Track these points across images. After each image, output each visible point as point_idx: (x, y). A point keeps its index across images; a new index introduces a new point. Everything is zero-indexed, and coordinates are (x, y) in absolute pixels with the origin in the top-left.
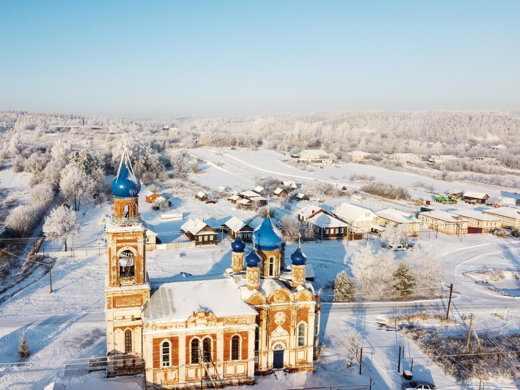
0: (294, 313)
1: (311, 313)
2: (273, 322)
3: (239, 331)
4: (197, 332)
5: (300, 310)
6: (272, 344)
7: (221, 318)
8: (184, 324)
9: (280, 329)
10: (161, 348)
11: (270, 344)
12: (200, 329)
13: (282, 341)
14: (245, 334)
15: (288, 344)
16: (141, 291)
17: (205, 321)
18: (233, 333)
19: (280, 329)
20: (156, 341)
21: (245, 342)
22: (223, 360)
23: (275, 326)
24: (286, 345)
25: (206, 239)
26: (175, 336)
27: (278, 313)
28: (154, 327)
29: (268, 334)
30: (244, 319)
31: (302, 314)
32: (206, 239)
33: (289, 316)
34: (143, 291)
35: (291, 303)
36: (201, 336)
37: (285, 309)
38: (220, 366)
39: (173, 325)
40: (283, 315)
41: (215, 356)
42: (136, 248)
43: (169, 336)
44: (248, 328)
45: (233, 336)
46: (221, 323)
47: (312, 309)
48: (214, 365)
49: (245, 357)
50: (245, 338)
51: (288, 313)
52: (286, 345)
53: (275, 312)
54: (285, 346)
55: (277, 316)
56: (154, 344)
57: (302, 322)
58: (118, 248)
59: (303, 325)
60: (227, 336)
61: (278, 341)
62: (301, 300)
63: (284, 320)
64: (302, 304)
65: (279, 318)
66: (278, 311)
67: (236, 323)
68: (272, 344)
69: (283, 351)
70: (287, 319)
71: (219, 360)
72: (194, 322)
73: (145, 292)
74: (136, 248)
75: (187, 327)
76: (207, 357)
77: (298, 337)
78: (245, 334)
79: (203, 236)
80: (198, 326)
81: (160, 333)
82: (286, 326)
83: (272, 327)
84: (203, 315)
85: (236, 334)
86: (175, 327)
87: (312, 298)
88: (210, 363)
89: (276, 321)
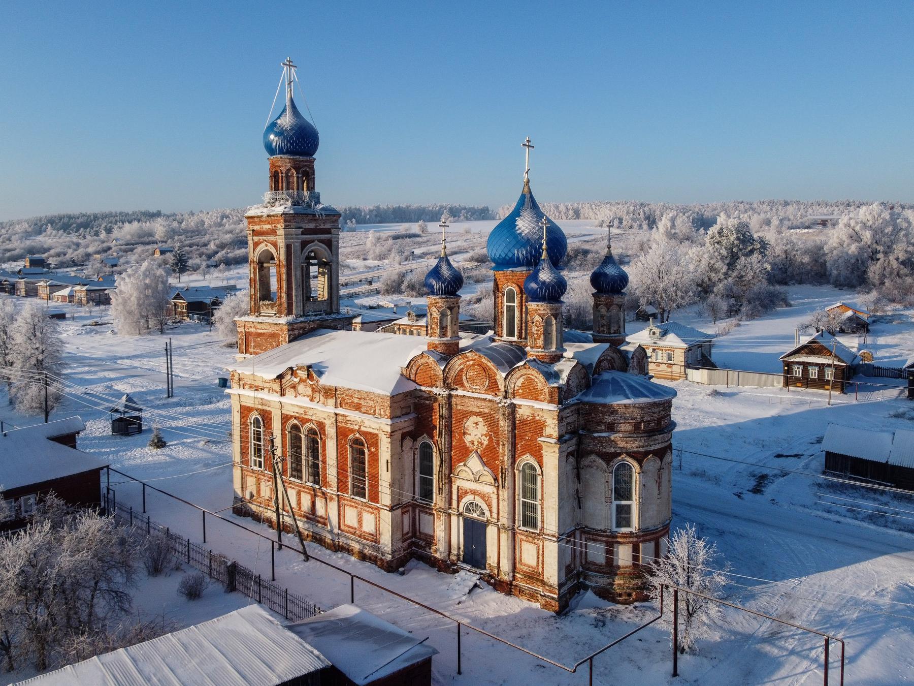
0: (504, 425)
1: (550, 436)
2: (461, 440)
3: (363, 429)
4: (296, 410)
5: (524, 422)
6: (459, 499)
7: (330, 390)
8: (276, 387)
9: (474, 463)
10: (252, 429)
11: (455, 497)
12: (296, 403)
13: (483, 496)
14: (373, 439)
15: (495, 510)
16: (277, 328)
17: (309, 391)
18: (352, 431)
19: (474, 463)
20: (245, 411)
21: (375, 458)
22: (336, 489)
23: (465, 453)
24: (491, 511)
25: (813, 373)
26: (268, 409)
27: (473, 419)
28: (241, 383)
29: (450, 467)
30: (371, 403)
31: (521, 434)
32: (813, 373)
33: (496, 433)
34: (279, 328)
35: (497, 399)
36: (304, 421)
37: (486, 411)
38: (331, 499)
39: (266, 385)
40: (483, 429)
41: (325, 477)
42: (275, 245)
43: (260, 407)
44: (377, 426)
45: (351, 436)
46: (331, 401)
47: (552, 429)
48: (323, 493)
49: (375, 498)
50: (373, 450)
51: (490, 420)
52: (491, 511)
53: (467, 415)
54: (487, 513)
55: (470, 423)
56: (241, 417)
57: (528, 459)
58: (256, 245)
59: (532, 468)
60: (342, 433)
61: (474, 493)
62: (524, 396)
63: (486, 443)
64: (526, 407)
65: (475, 432)
66: (472, 413)
67: (358, 407)
68: (459, 499)
69: (483, 526)
70: (490, 440)
71: (330, 485)
72: (294, 387)
73: (282, 330)
74: (275, 245)
75: (282, 394)
76: (316, 474)
77: (520, 499)
78: (373, 439)
79: (806, 365)
80: (299, 397)
81: (249, 397)
82: (489, 457)
83: (456, 454)
84: (303, 374)
85: (358, 435)
86: (266, 390)
87: (551, 394)
88: (317, 487)
89: (468, 439)
